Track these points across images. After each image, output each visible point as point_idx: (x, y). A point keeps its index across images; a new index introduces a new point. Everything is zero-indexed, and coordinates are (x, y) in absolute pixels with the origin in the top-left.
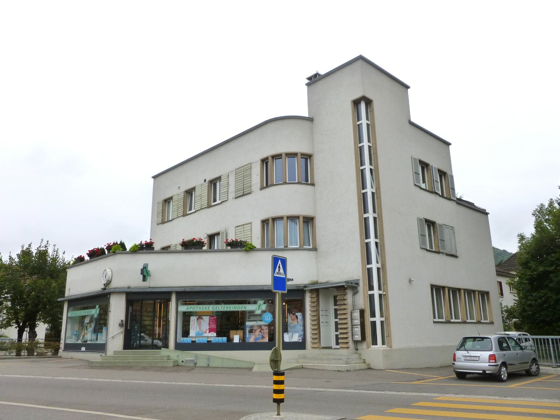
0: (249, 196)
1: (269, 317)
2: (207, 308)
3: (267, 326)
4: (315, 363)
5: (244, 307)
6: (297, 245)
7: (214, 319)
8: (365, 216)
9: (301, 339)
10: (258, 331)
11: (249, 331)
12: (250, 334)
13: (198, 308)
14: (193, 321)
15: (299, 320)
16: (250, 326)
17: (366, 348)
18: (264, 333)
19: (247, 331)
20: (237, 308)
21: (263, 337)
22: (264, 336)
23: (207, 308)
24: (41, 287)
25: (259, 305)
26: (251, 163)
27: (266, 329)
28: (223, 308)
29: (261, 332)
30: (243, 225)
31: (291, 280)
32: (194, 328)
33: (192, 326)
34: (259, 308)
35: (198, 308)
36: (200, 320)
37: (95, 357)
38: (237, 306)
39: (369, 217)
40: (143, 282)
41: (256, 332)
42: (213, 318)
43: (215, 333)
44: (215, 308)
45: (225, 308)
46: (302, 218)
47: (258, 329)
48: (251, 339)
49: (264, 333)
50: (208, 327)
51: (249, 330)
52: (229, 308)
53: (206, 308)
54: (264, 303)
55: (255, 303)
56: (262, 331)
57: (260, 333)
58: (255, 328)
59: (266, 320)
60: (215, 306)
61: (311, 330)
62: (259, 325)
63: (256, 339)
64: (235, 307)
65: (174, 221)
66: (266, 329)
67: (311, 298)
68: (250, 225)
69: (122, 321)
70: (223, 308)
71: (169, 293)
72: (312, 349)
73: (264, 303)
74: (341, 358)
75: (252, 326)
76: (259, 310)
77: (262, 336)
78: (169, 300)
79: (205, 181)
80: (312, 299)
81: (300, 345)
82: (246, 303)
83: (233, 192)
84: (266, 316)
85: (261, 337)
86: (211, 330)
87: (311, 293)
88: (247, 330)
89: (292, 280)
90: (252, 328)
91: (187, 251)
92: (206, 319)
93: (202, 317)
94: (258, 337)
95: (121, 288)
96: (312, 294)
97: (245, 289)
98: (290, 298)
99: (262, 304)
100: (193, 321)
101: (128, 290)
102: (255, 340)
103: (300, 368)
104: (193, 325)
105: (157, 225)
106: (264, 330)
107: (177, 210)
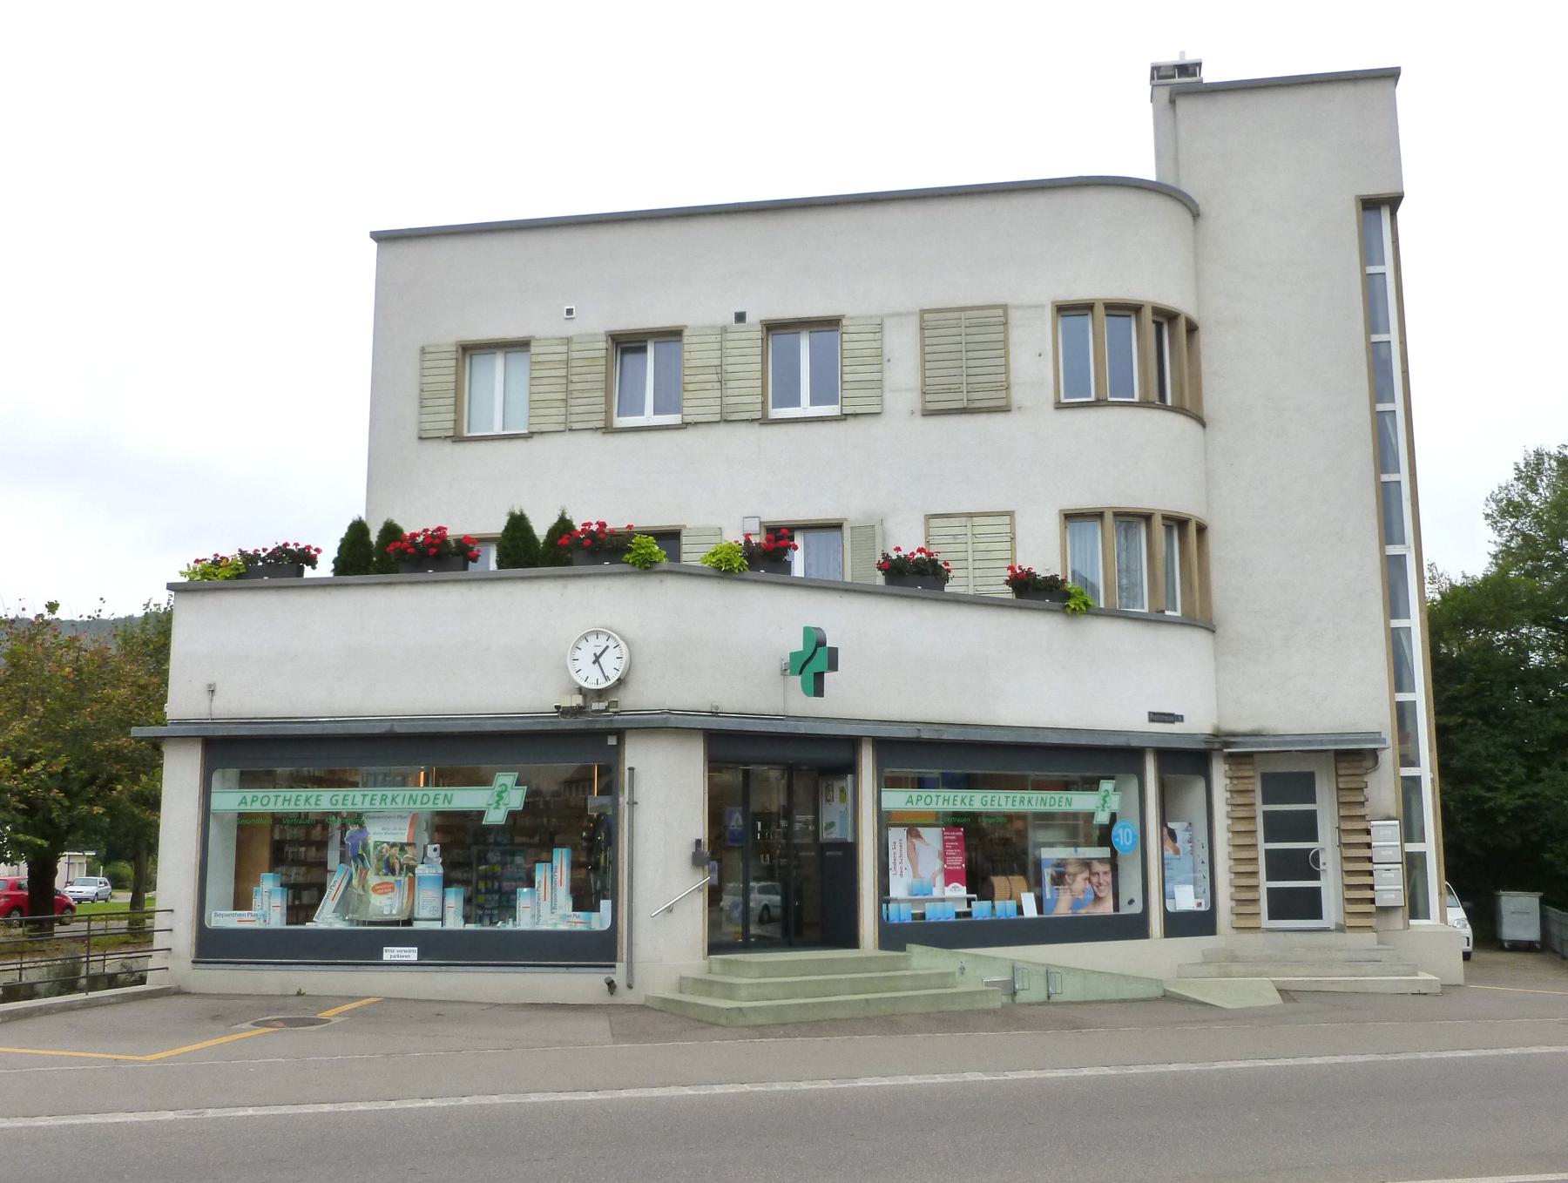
0: (998, 419)
1: (1128, 833)
2: (312, 801)
3: (1106, 863)
4: (1297, 974)
5: (446, 795)
6: (1143, 608)
7: (957, 836)
8: (1393, 550)
9: (1203, 904)
10: (1080, 878)
11: (1053, 879)
12: (1057, 889)
13: (280, 800)
14: (898, 845)
15: (1178, 844)
16: (1055, 862)
17: (1402, 928)
18: (1100, 884)
19: (1047, 880)
20: (951, 802)
21: (1097, 899)
22: (1100, 895)
23: (312, 801)
24: (1484, 728)
25: (498, 789)
26: (1006, 305)
27: (1105, 873)
28: (368, 799)
29: (1090, 882)
30: (970, 515)
31: (1180, 718)
32: (901, 868)
33: (895, 863)
34: (497, 802)
35: (280, 800)
36: (914, 840)
37: (583, 984)
38: (1049, 796)
39: (1105, 514)
40: (1147, 716)
41: (1074, 881)
42: (954, 835)
43: (963, 885)
44: (340, 801)
45: (440, 802)
46: (1160, 518)
47: (1081, 872)
48: (1062, 907)
49: (1100, 884)
50: (938, 864)
51: (1052, 875)
52: (1026, 802)
53: (307, 800)
54: (518, 783)
55: (482, 781)
56: (1095, 879)
57: (1088, 886)
58: (1071, 869)
59: (1122, 843)
60: (915, 793)
61: (1233, 876)
62: (1083, 859)
63: (1077, 904)
64: (411, 796)
65: (536, 443)
66: (1105, 873)
67: (1231, 778)
68: (1007, 519)
69: (698, 842)
70: (368, 799)
71: (853, 743)
72: (1234, 931)
73: (518, 783)
74: (1378, 958)
75: (1061, 864)
76: (497, 808)
77: (1095, 894)
78: (852, 768)
79: (740, 317)
80: (1235, 782)
81: (1198, 924)
82: (1024, 788)
83: (908, 390)
84: (1120, 831)
85: (1092, 897)
86: (950, 877)
87: (1230, 764)
88: (1047, 873)
89: (1179, 718)
90: (1062, 869)
91: (1022, 602)
92: (933, 837)
93: (919, 829)
94: (1081, 897)
95: (685, 713)
96: (1234, 768)
97: (489, 727)
98: (948, 771)
99: (509, 789)
100: (898, 845)
101: (714, 724)
102: (1071, 909)
103: (1157, 999)
104: (898, 860)
105: (415, 440)
106: (1098, 874)
107: (565, 400)
